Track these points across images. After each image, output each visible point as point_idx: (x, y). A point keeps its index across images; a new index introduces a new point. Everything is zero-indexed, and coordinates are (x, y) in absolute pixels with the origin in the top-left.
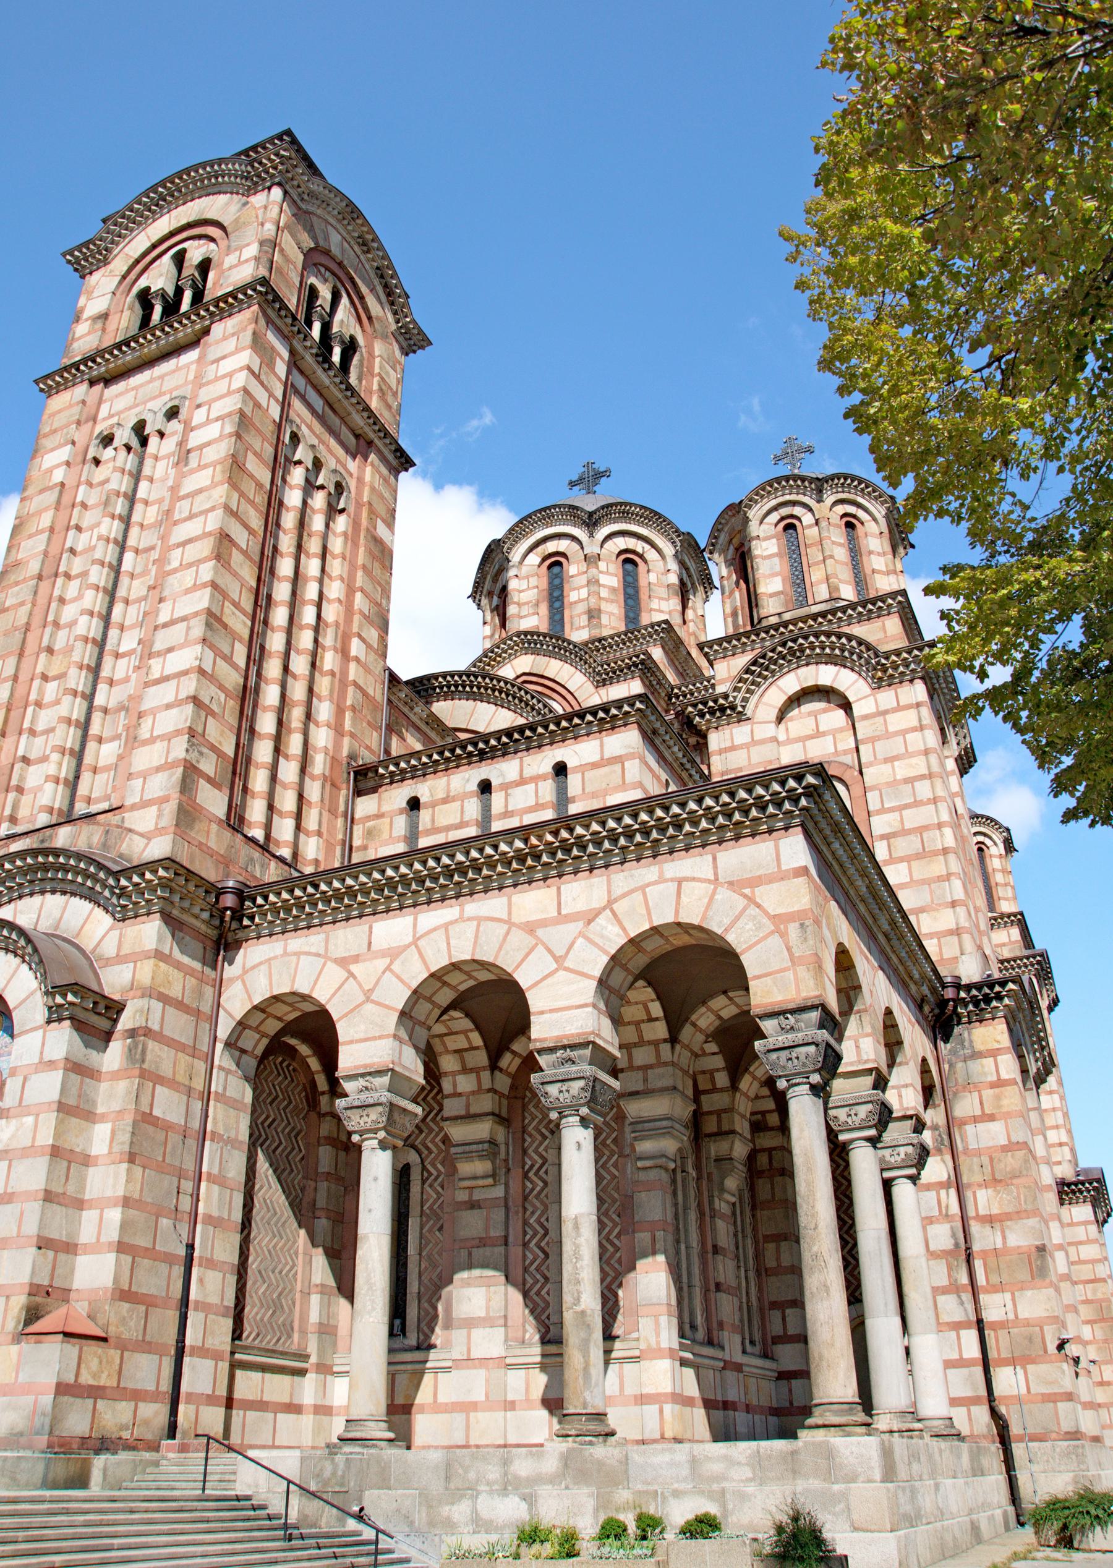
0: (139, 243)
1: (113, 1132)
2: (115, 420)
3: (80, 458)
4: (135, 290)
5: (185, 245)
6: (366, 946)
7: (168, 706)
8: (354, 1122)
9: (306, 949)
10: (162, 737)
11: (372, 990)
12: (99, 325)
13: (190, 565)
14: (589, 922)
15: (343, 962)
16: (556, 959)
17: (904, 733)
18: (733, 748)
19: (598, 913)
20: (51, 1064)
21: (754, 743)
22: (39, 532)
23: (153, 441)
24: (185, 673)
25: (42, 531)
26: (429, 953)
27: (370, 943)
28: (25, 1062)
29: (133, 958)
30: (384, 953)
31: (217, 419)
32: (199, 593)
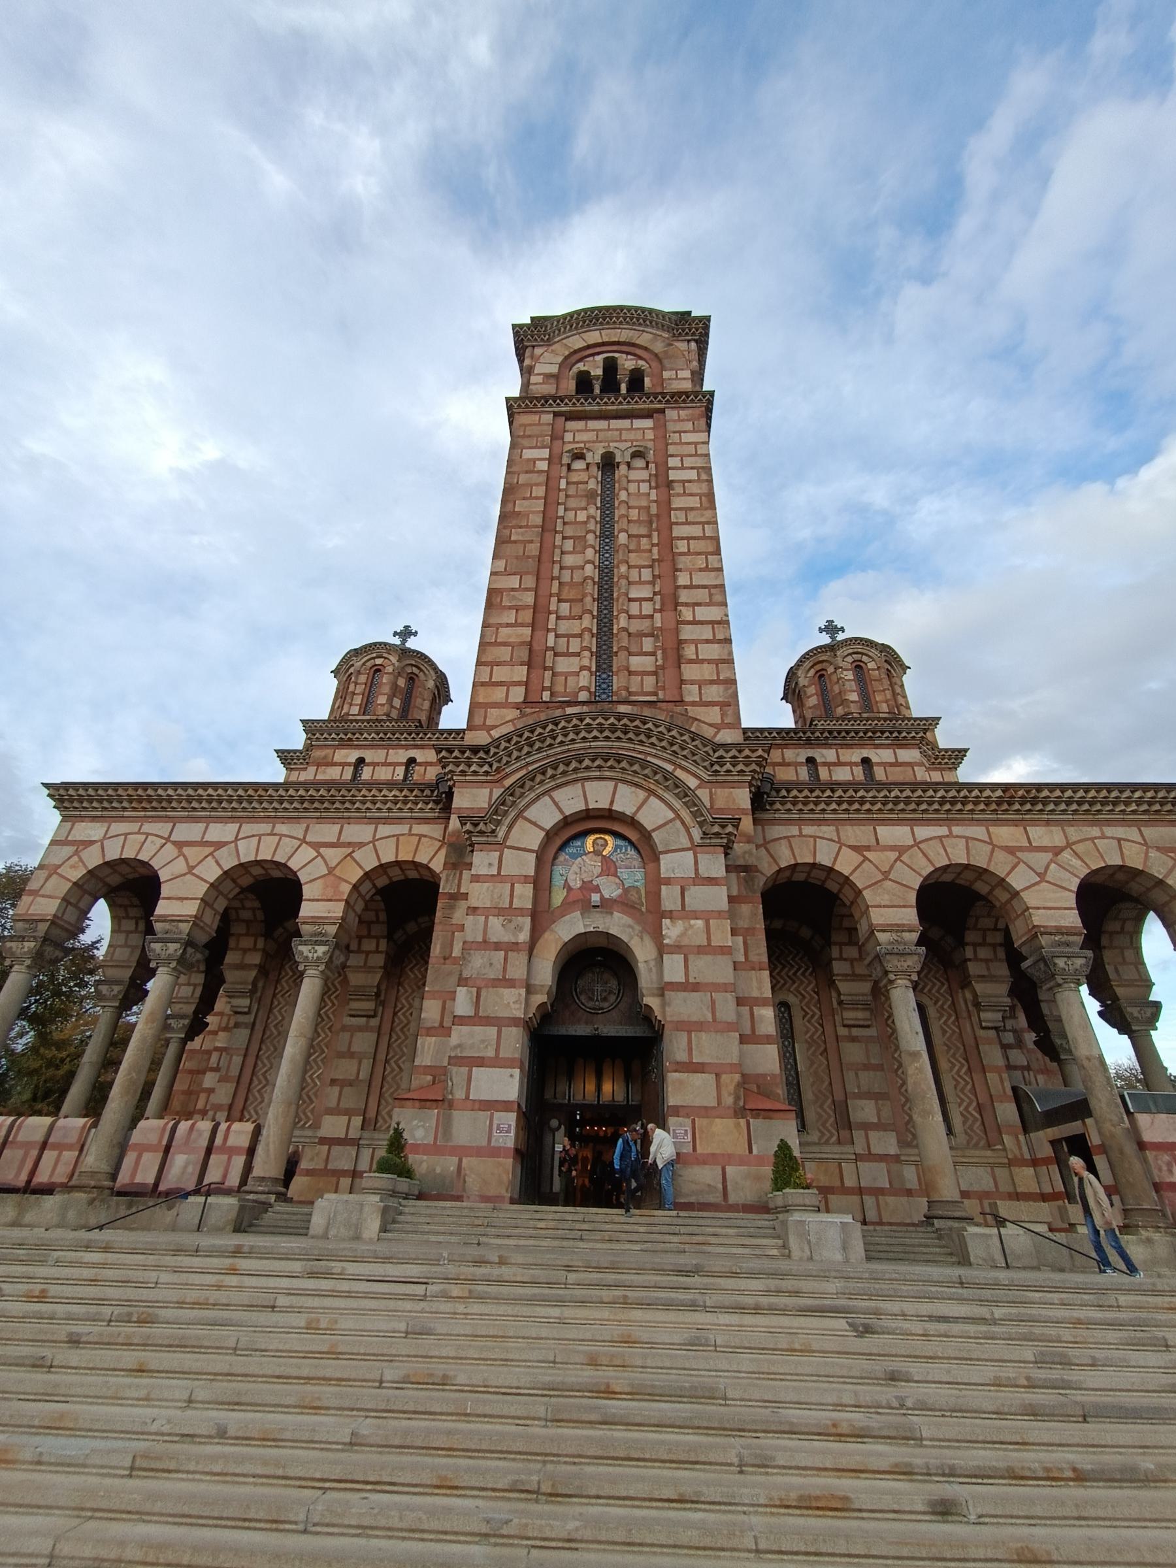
0: (576, 342)
1: (745, 943)
3: (556, 460)
4: (575, 370)
5: (616, 355)
6: (874, 841)
7: (707, 641)
8: (892, 964)
9: (821, 835)
10: (709, 661)
11: (889, 872)
12: (552, 381)
13: (699, 554)
14: (1057, 854)
16: (1038, 874)
19: (1062, 849)
20: (712, 881)
22: (531, 497)
23: (623, 469)
25: (537, 498)
26: (931, 854)
27: (877, 840)
28: (678, 875)
30: (893, 848)
31: (692, 468)
32: (713, 574)
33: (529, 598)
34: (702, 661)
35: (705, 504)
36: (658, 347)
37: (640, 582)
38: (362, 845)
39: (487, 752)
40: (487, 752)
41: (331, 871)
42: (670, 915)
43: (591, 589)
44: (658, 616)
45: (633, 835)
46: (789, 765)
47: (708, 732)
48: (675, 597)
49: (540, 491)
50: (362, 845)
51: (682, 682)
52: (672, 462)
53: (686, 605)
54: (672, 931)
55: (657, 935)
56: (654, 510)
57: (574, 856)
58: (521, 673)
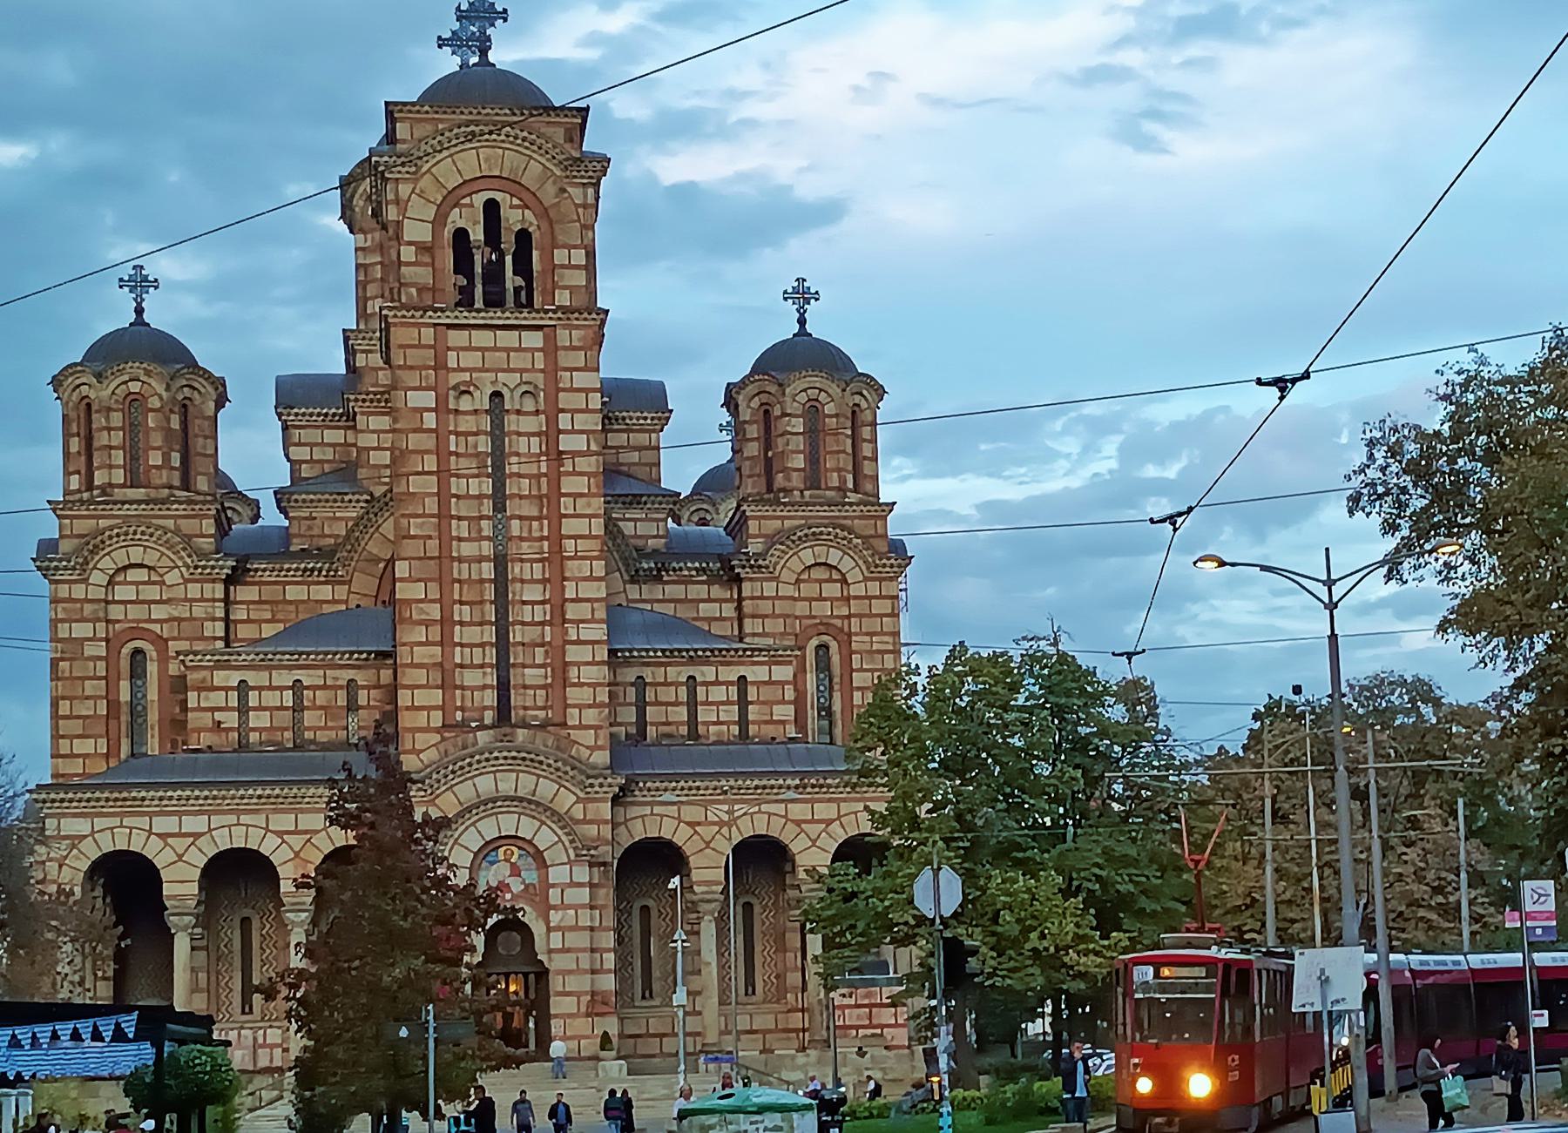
2: (466, 376)
7: (588, 664)
10: (588, 685)
15: (688, 824)
17: (881, 616)
18: (762, 598)
21: (777, 597)
24: (598, 642)
29: (598, 822)
33: (435, 612)
34: (582, 685)
35: (594, 490)
36: (548, 194)
37: (533, 581)
38: (318, 832)
39: (423, 783)
40: (423, 783)
41: (297, 854)
42: (555, 908)
43: (489, 593)
44: (547, 628)
45: (531, 850)
46: (671, 684)
47: (585, 753)
48: (563, 613)
49: (431, 463)
50: (318, 832)
51: (567, 706)
52: (564, 421)
53: (571, 621)
54: (555, 918)
55: (547, 922)
56: (544, 491)
57: (492, 863)
58: (436, 696)
